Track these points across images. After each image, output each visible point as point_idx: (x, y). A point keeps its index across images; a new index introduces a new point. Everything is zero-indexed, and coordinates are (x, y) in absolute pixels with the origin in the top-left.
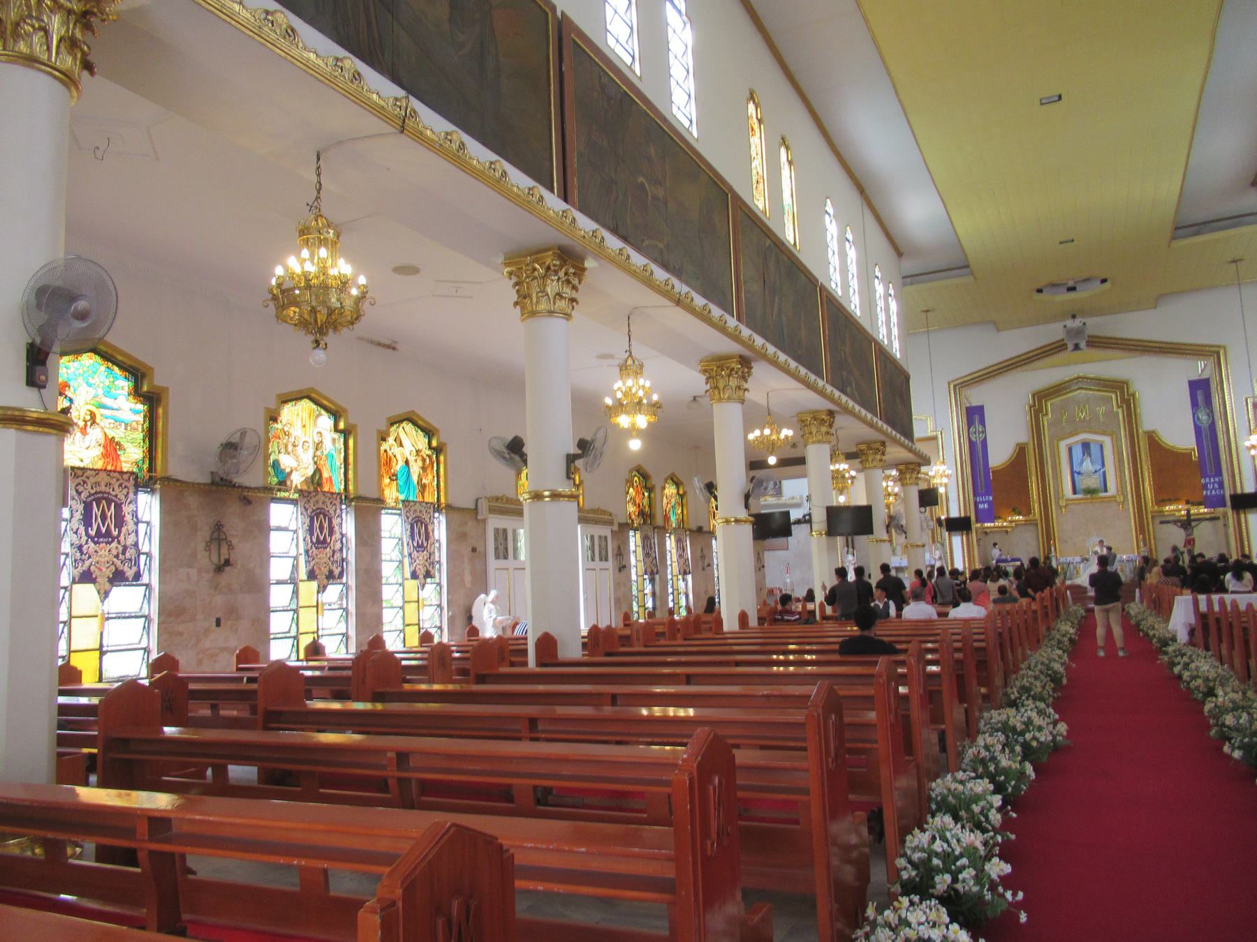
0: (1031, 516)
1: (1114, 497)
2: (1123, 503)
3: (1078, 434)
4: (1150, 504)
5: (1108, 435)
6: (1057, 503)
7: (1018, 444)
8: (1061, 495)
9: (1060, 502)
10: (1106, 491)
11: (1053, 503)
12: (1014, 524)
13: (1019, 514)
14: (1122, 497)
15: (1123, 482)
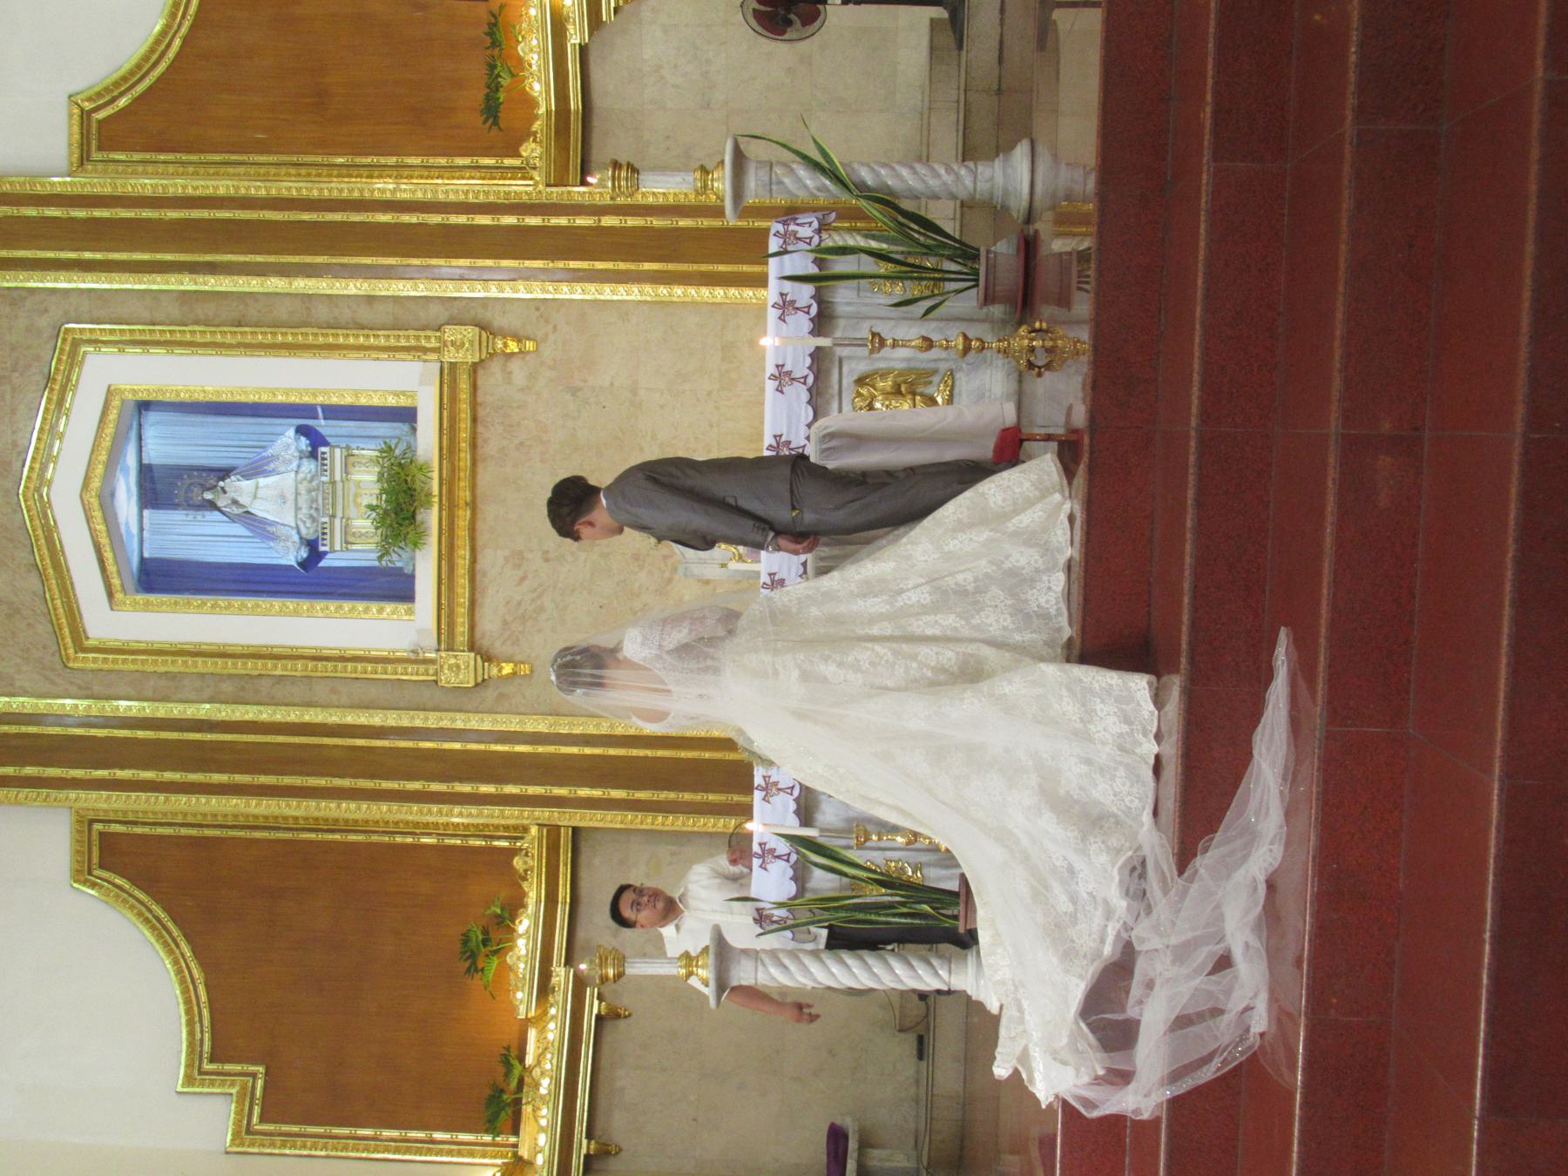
0: (529, 862)
1: (448, 375)
2: (483, 326)
3: (50, 532)
4: (519, 188)
5: (74, 360)
6: (459, 699)
7: (82, 873)
8: (412, 674)
9: (448, 678)
10: (407, 415)
11: (460, 722)
12: (561, 975)
13: (502, 924)
14: (451, 333)
15: (364, 314)
